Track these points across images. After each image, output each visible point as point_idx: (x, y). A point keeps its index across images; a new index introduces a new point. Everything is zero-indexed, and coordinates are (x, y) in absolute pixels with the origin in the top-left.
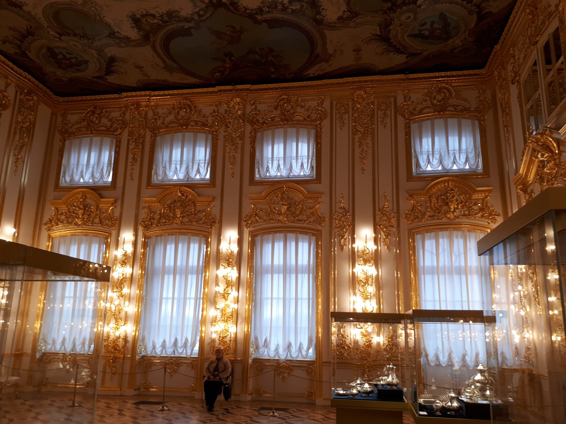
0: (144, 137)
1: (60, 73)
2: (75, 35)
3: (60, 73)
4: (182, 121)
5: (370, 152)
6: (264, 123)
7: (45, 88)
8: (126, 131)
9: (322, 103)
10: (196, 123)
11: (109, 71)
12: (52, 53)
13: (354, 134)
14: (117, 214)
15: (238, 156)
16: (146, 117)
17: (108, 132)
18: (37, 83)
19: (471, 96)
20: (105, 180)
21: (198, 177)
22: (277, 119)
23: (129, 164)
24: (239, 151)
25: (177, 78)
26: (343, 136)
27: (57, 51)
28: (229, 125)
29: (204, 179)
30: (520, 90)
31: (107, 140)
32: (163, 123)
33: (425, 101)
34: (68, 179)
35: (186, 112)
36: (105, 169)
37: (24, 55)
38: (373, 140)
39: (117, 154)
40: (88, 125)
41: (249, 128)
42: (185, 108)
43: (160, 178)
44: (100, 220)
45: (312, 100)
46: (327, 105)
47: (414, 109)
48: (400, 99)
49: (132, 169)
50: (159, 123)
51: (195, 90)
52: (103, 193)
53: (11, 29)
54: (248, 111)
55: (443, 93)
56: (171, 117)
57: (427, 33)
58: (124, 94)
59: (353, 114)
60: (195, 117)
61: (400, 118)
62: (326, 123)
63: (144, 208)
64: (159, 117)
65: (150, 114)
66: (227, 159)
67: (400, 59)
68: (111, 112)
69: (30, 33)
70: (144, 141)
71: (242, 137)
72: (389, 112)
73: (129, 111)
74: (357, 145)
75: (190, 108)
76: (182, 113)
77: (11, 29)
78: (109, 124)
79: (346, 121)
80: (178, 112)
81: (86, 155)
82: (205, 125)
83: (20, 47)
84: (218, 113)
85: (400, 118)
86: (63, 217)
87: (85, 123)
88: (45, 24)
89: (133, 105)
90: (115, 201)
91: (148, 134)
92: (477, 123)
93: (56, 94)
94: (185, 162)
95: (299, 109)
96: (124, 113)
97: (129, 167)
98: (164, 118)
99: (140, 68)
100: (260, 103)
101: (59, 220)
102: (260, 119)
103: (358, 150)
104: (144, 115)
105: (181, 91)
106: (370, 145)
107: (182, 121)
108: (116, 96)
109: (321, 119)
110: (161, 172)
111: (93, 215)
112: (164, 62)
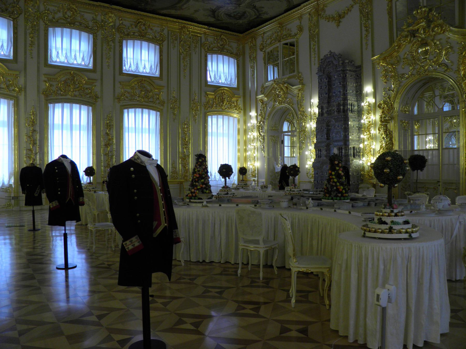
4: (69, 20)
9: (163, 30)
13: (180, 54)
19: (234, 45)
22: (136, 34)
24: (112, 50)
30: (265, 55)
33: (215, 43)
38: (190, 60)
47: (210, 47)
48: (203, 40)
49: (31, 50)
55: (223, 41)
57: (233, 15)
59: (180, 42)
61: (203, 50)
62: (165, 43)
67: (212, 20)
72: (198, 45)
74: (182, 61)
79: (176, 45)
82: (87, 27)
85: (203, 50)
92: (236, 61)
95: (149, 31)
97: (28, 48)
106: (188, 62)
109: (163, 41)
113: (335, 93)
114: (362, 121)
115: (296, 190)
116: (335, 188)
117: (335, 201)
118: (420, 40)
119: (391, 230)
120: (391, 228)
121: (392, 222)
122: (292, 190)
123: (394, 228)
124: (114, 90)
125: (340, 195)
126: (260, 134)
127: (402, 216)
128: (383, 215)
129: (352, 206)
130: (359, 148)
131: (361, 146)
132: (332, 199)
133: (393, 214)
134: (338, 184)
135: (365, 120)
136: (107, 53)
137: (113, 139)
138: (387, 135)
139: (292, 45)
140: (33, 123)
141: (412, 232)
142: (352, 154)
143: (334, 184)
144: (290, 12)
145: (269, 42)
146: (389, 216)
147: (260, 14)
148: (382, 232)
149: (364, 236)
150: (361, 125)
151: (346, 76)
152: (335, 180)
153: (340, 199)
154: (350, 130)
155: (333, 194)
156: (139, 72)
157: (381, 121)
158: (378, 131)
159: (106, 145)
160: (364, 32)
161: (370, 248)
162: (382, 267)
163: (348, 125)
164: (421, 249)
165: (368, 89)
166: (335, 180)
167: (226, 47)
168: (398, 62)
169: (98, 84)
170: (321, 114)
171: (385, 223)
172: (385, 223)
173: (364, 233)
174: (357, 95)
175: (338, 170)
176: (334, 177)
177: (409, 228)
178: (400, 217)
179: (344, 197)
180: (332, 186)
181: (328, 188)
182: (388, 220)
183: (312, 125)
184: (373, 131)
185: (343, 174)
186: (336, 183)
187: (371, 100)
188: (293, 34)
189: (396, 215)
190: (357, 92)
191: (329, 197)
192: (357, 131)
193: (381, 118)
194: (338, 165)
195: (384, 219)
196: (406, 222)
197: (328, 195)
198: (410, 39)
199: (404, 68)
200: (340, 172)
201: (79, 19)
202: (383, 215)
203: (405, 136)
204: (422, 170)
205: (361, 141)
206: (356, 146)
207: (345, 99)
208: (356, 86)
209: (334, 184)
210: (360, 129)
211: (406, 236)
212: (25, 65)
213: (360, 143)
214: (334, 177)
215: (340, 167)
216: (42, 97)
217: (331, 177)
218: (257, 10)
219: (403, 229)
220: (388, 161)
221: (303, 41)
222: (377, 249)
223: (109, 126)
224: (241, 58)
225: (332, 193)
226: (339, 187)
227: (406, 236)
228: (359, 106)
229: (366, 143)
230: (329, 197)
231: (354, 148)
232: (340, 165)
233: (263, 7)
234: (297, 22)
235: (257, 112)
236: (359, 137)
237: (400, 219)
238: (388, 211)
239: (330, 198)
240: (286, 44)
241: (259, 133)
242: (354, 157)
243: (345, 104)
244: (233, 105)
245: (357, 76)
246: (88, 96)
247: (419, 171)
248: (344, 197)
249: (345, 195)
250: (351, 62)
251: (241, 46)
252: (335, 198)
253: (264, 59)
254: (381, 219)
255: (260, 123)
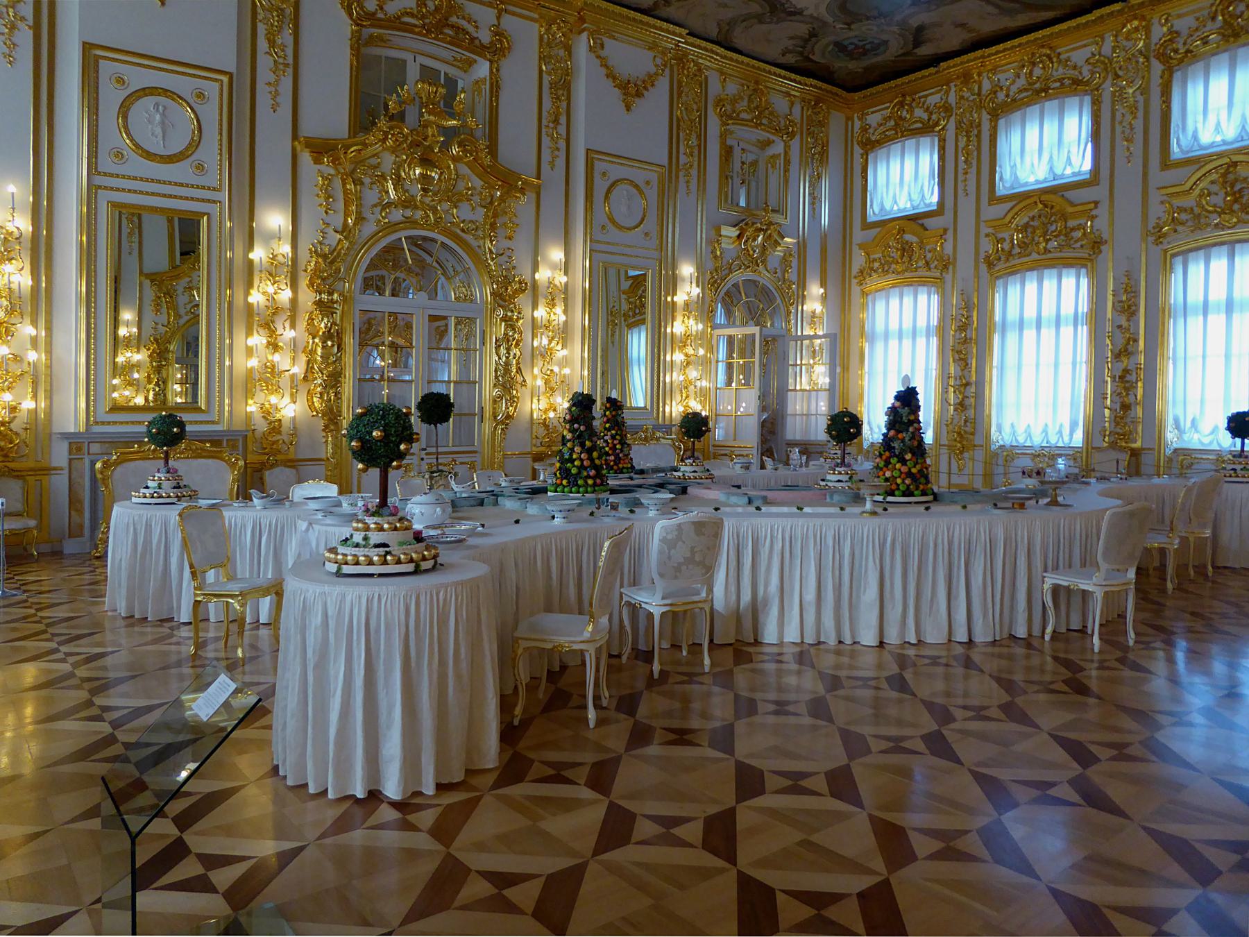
0: (979, 125)
1: (852, 65)
2: (868, 18)
3: (852, 65)
4: (1038, 85)
6: (1188, 51)
7: (835, 89)
8: (953, 119)
10: (1061, 80)
11: (917, 43)
12: (840, 47)
14: (949, 249)
15: (1138, 124)
16: (979, 94)
17: (926, 129)
18: (825, 86)
20: (927, 202)
21: (1068, 171)
23: (960, 171)
25: (1022, 20)
27: (846, 43)
28: (1120, 73)
29: (1079, 173)
31: (925, 141)
32: (1007, 96)
34: (876, 209)
35: (1044, 68)
36: (926, 184)
37: (808, 59)
39: (942, 158)
40: (897, 124)
41: (1157, 67)
42: (1041, 62)
43: (1008, 185)
44: (927, 263)
50: (1001, 96)
51: (1057, 28)
52: (927, 222)
53: (791, 38)
54: (1154, 39)
56: (1022, 82)
58: (943, 65)
60: (1059, 72)
63: (987, 235)
64: (1001, 88)
65: (986, 86)
66: (1118, 129)
68: (926, 96)
69: (813, 34)
70: (980, 132)
71: (1144, 91)
73: (953, 89)
75: (1050, 59)
76: (1038, 71)
77: (791, 38)
78: (925, 116)
80: (1031, 72)
81: (898, 166)
83: (801, 54)
84: (1100, 54)
86: (876, 265)
87: (892, 123)
88: (830, 20)
89: (958, 78)
90: (945, 230)
91: (985, 117)
93: (849, 90)
94: (1047, 148)
96: (947, 92)
97: (961, 177)
98: (1008, 89)
99: (963, 25)
100: (1179, 16)
101: (872, 269)
102: (1180, 46)
104: (976, 91)
105: (1032, 36)
107: (1038, 85)
108: (932, 70)
110: (1007, 175)
111: (916, 257)
112: (997, 6)
124: (1145, 216)
136: (968, 162)
137: (1136, 341)
140: (963, 328)
156: (1202, 148)
159: (1117, 356)
169: (1102, 211)
201: (1061, 70)
212: (956, 212)
216: (983, 267)
223: (1128, 309)
246: (1078, 245)
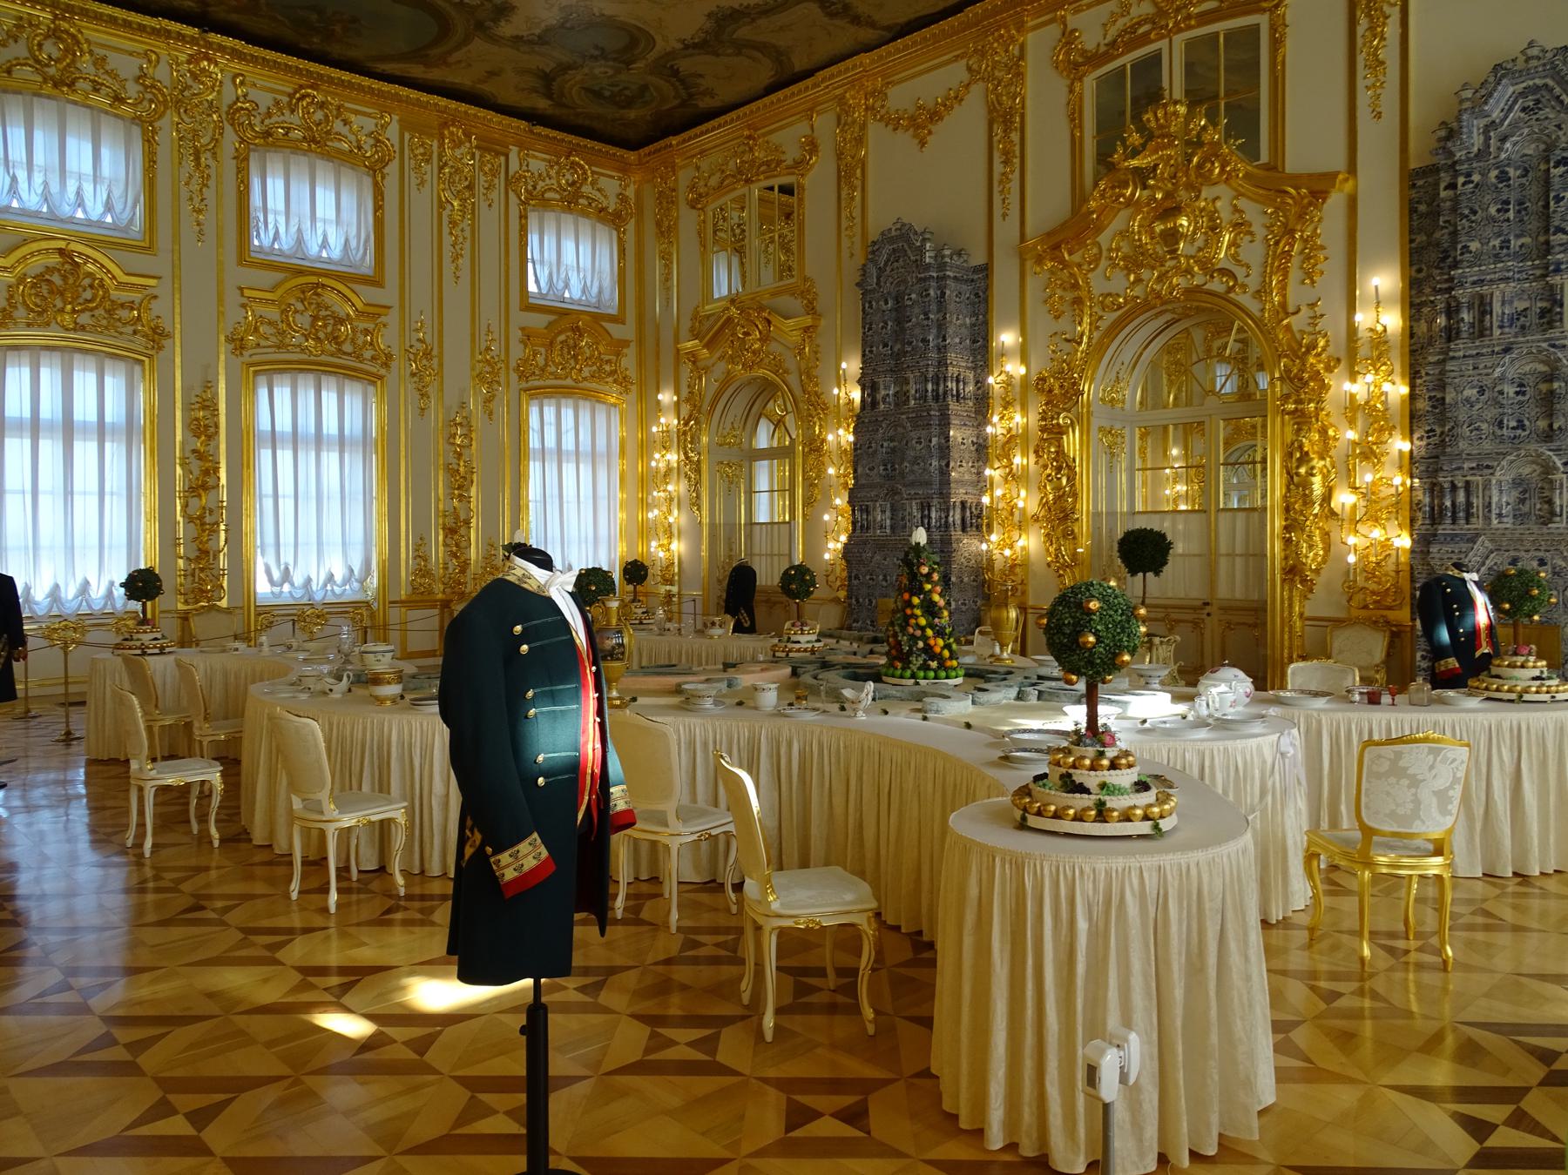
5: (467, 245)
13: (441, 206)
26: (422, 203)
45: (368, 115)
46: (393, 132)
47: (535, 188)
48: (514, 165)
57: (607, 94)
59: (441, 168)
61: (512, 195)
62: (392, 169)
67: (542, 104)
74: (446, 230)
85: (512, 195)
95: (338, 126)
103: (448, 240)
106: (467, 234)
113: (910, 343)
114: (989, 429)
115: (803, 639)
116: (921, 644)
117: (923, 682)
118: (1159, 196)
119: (1102, 814)
120: (1100, 805)
121: (1103, 786)
122: (794, 638)
123: (1109, 805)
125: (934, 664)
126: (687, 458)
127: (1130, 766)
128: (1074, 766)
129: (974, 702)
130: (979, 504)
131: (986, 500)
132: (913, 676)
133: (1105, 762)
134: (929, 632)
135: (996, 428)
138: (1059, 469)
139: (787, 190)
141: (1162, 817)
142: (958, 522)
143: (918, 633)
144: (780, 94)
145: (714, 182)
146: (1093, 768)
147: (691, 96)
148: (1078, 818)
149: (1022, 826)
150: (986, 440)
151: (943, 294)
152: (923, 622)
153: (936, 678)
154: (954, 454)
155: (917, 661)
157: (1043, 429)
158: (1032, 458)
160: (998, 168)
161: (1046, 871)
162: (1082, 925)
163: (947, 438)
164: (1194, 872)
165: (1007, 338)
166: (923, 622)
167: (586, 189)
168: (1096, 260)
170: (869, 403)
171: (1082, 789)
172: (1082, 789)
173: (1024, 819)
174: (973, 352)
175: (930, 591)
176: (918, 612)
177: (1151, 805)
178: (1125, 771)
179: (946, 669)
180: (914, 638)
181: (899, 643)
182: (1091, 780)
183: (843, 436)
184: (1018, 460)
185: (942, 603)
186: (923, 629)
187: (1016, 369)
188: (789, 162)
189: (1114, 766)
190: (975, 341)
191: (904, 669)
192: (974, 455)
193: (1043, 419)
194: (928, 576)
195: (1080, 776)
196: (1142, 786)
197: (899, 665)
198: (1133, 194)
199: (1108, 279)
200: (936, 598)
202: (1074, 766)
203: (1111, 470)
204: (1157, 573)
205: (982, 485)
206: (970, 499)
207: (942, 363)
208: (973, 325)
209: (918, 633)
210: (982, 452)
211: (1145, 828)
213: (982, 492)
214: (918, 612)
215: (935, 584)
217: (909, 611)
218: (682, 82)
219: (1135, 807)
220: (1090, 612)
221: (818, 181)
222: (1069, 873)
224: (631, 226)
225: (913, 659)
226: (932, 642)
227: (1145, 828)
228: (980, 383)
229: (998, 492)
230: (904, 669)
231: (963, 504)
232: (936, 577)
233: (701, 76)
234: (802, 128)
235: (677, 392)
236: (979, 474)
237: (1125, 778)
238: (1090, 751)
239: (908, 673)
240: (771, 189)
241: (686, 454)
242: (964, 529)
243: (939, 379)
244: (607, 368)
245: (977, 295)
247: (1150, 575)
248: (946, 669)
249: (949, 663)
250: (959, 255)
251: (630, 192)
252: (922, 674)
253: (700, 233)
254: (1070, 775)
255: (686, 424)
